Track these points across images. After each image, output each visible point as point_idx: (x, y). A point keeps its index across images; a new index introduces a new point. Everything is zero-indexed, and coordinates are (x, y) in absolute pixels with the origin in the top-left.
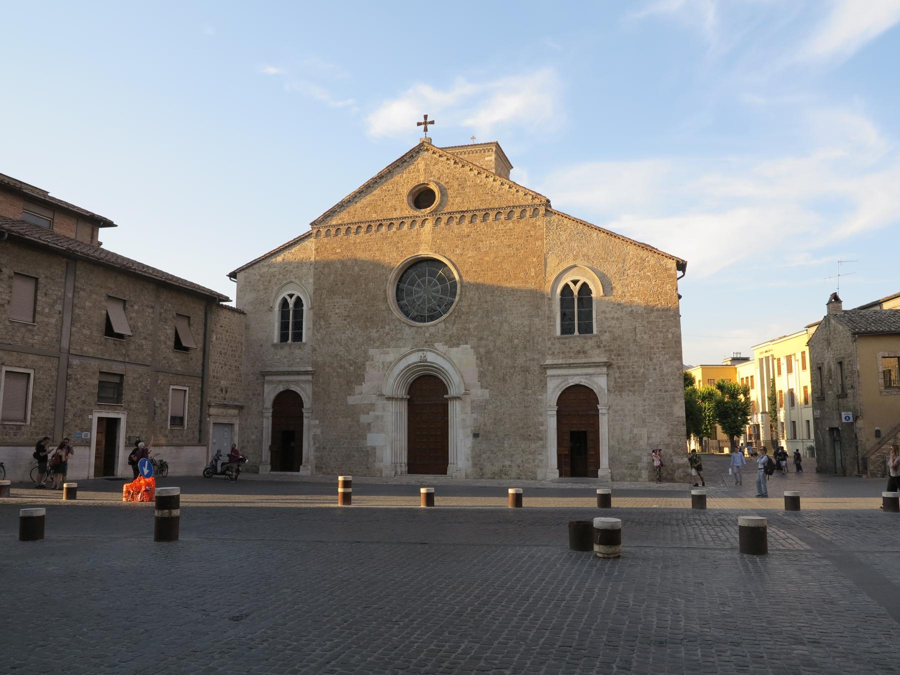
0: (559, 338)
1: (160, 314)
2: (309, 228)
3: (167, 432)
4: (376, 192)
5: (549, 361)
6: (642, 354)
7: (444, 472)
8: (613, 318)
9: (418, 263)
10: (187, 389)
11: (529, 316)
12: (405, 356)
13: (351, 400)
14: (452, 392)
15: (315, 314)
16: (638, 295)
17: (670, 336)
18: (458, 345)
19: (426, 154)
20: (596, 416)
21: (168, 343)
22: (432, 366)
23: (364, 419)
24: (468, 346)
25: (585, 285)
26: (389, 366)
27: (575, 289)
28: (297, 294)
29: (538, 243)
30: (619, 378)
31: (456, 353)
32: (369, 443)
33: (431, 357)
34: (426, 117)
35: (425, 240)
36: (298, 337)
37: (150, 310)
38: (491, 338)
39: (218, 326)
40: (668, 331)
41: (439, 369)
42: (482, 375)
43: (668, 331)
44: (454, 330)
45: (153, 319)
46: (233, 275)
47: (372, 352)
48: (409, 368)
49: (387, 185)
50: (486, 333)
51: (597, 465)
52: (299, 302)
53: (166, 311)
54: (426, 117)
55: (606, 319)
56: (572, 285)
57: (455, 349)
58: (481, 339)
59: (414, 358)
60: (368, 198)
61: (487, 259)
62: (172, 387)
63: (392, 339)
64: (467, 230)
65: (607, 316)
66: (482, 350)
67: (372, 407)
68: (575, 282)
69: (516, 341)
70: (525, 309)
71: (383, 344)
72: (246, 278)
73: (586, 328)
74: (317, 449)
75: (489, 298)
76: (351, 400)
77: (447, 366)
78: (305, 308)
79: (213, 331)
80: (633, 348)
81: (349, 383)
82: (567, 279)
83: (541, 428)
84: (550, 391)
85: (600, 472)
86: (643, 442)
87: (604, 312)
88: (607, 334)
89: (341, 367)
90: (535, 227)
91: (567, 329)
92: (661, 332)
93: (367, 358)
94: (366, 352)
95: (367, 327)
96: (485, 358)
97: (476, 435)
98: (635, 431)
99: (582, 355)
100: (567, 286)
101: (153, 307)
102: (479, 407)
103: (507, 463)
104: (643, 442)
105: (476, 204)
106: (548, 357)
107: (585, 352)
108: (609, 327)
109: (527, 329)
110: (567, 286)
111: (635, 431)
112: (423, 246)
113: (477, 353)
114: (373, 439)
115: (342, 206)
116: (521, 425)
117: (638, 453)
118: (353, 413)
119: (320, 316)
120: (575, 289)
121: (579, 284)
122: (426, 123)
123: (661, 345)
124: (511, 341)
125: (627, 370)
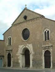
0: (44, 42)
7: (29, 67)
9: (26, 29)
12: (23, 47)
13: (17, 55)
14: (30, 52)
19: (25, 10)
20: (50, 56)
22: (27, 48)
23: (18, 58)
25: (48, 31)
26: (21, 48)
27: (47, 32)
31: (30, 45)
33: (26, 47)
35: (25, 26)
36: (10, 44)
41: (28, 48)
46: (3, 35)
47: (19, 46)
48: (24, 48)
51: (51, 66)
52: (10, 38)
59: (24, 47)
60: (18, 19)
67: (19, 55)
68: (47, 30)
73: (48, 39)
74: (13, 63)
76: (17, 55)
77: (29, 48)
85: (51, 67)
91: (46, 40)
97: (33, 60)
100: (45, 31)
105: (32, 18)
110: (45, 31)
114: (20, 61)
118: (17, 56)
120: (47, 32)
122: (26, 5)
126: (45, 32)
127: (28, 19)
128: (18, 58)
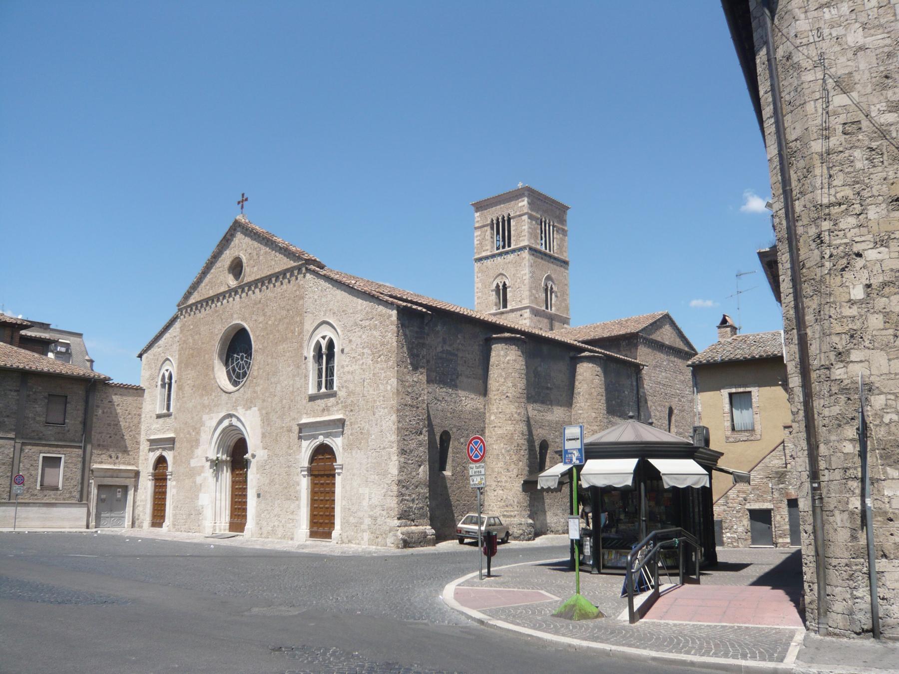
1: (29, 396)
2: (174, 311)
3: (36, 492)
4: (212, 271)
5: (304, 420)
6: (368, 409)
8: (348, 372)
10: (63, 456)
11: (294, 376)
15: (178, 386)
16: (367, 347)
17: (389, 388)
18: (250, 408)
21: (38, 418)
24: (256, 409)
27: (324, 343)
28: (170, 369)
29: (301, 302)
30: (351, 434)
32: (200, 503)
34: (243, 195)
37: (16, 394)
38: (270, 400)
39: (106, 402)
40: (387, 383)
42: (264, 436)
43: (387, 383)
44: (249, 394)
45: (18, 400)
47: (205, 417)
49: (218, 264)
50: (267, 394)
53: (35, 393)
54: (243, 195)
55: (344, 373)
56: (321, 341)
57: (248, 412)
58: (264, 401)
59: (226, 423)
60: (209, 276)
61: (270, 322)
62: (42, 455)
63: (215, 406)
64: (259, 297)
65: (346, 369)
66: (264, 412)
68: (324, 338)
69: (284, 401)
70: (291, 368)
71: (211, 411)
72: (147, 357)
75: (270, 361)
76: (193, 463)
78: (173, 381)
79: (98, 406)
80: (362, 403)
81: (192, 446)
82: (317, 337)
83: (298, 488)
84: (303, 450)
86: (365, 503)
87: (343, 367)
88: (344, 390)
89: (189, 433)
90: (299, 286)
92: (382, 384)
93: (203, 424)
94: (201, 419)
95: (203, 395)
96: (266, 420)
97: (259, 496)
98: (361, 491)
99: (326, 412)
100: (318, 342)
101: (16, 391)
102: (262, 467)
103: (276, 524)
104: (365, 503)
106: (305, 416)
107: (328, 410)
108: (345, 382)
109: (291, 389)
111: (361, 491)
112: (235, 316)
113: (261, 415)
115: (194, 287)
116: (285, 485)
117: (360, 514)
119: (180, 388)
121: (327, 339)
123: (381, 398)
124: (281, 401)
125: (356, 426)
126: (318, 347)
127: (251, 273)
128: (199, 480)
